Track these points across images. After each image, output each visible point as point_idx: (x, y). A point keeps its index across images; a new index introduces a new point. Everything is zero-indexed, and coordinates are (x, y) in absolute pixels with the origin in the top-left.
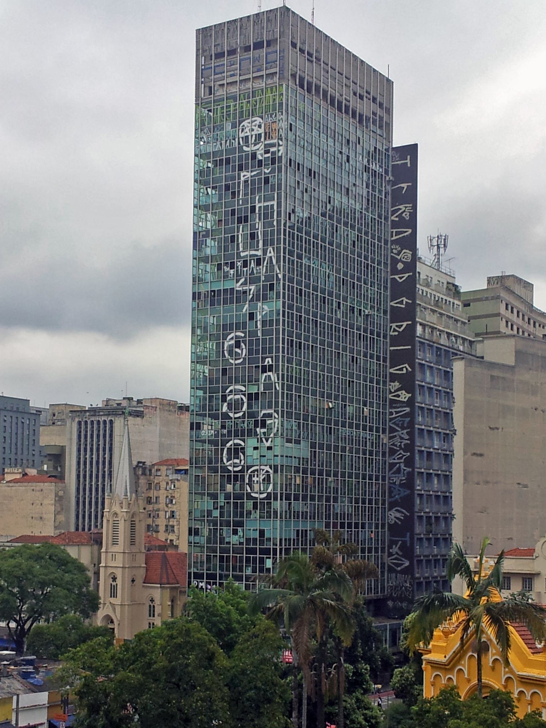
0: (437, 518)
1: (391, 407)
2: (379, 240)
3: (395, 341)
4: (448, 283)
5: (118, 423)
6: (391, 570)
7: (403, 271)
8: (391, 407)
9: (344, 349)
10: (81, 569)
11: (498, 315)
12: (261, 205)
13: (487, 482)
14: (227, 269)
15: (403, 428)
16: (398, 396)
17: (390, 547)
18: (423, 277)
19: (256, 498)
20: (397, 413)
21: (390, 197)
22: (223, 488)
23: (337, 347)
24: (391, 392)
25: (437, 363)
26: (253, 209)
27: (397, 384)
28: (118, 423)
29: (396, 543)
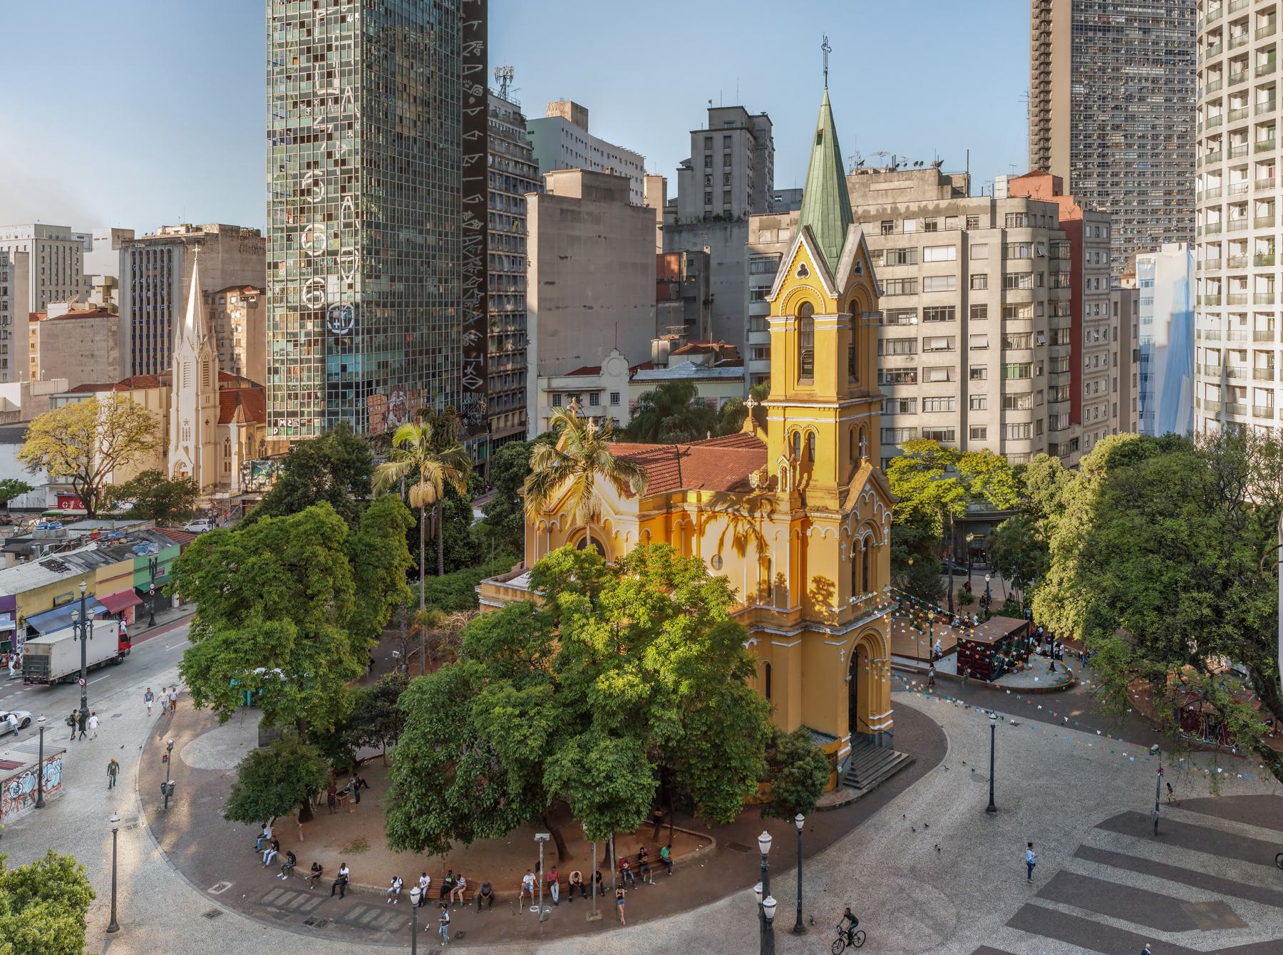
1: (465, 235)
2: (452, 76)
3: (468, 172)
4: (514, 113)
6: (466, 389)
7: (475, 105)
8: (465, 235)
9: (421, 183)
12: (338, 43)
14: (303, 107)
15: (476, 255)
16: (471, 225)
17: (465, 368)
19: (338, 335)
20: (470, 240)
21: (461, 34)
22: (302, 326)
23: (414, 182)
24: (464, 222)
25: (507, 190)
26: (329, 48)
27: (470, 214)
29: (470, 363)
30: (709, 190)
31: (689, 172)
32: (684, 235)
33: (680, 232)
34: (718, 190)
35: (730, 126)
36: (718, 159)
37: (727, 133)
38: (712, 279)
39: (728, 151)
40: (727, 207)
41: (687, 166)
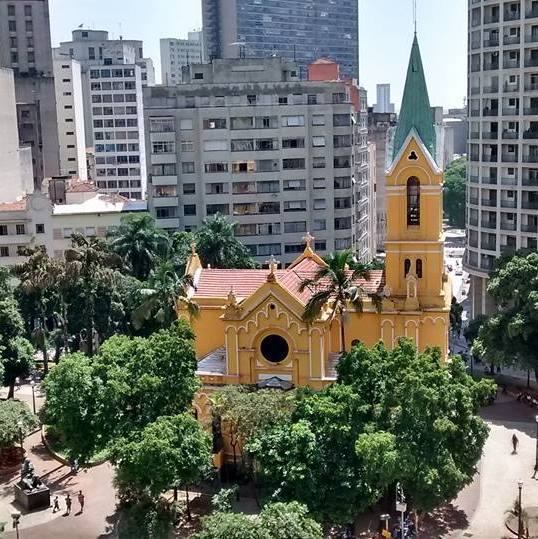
30: (14, 50)
36: (21, 25)
39: (29, 18)
40: (31, 65)
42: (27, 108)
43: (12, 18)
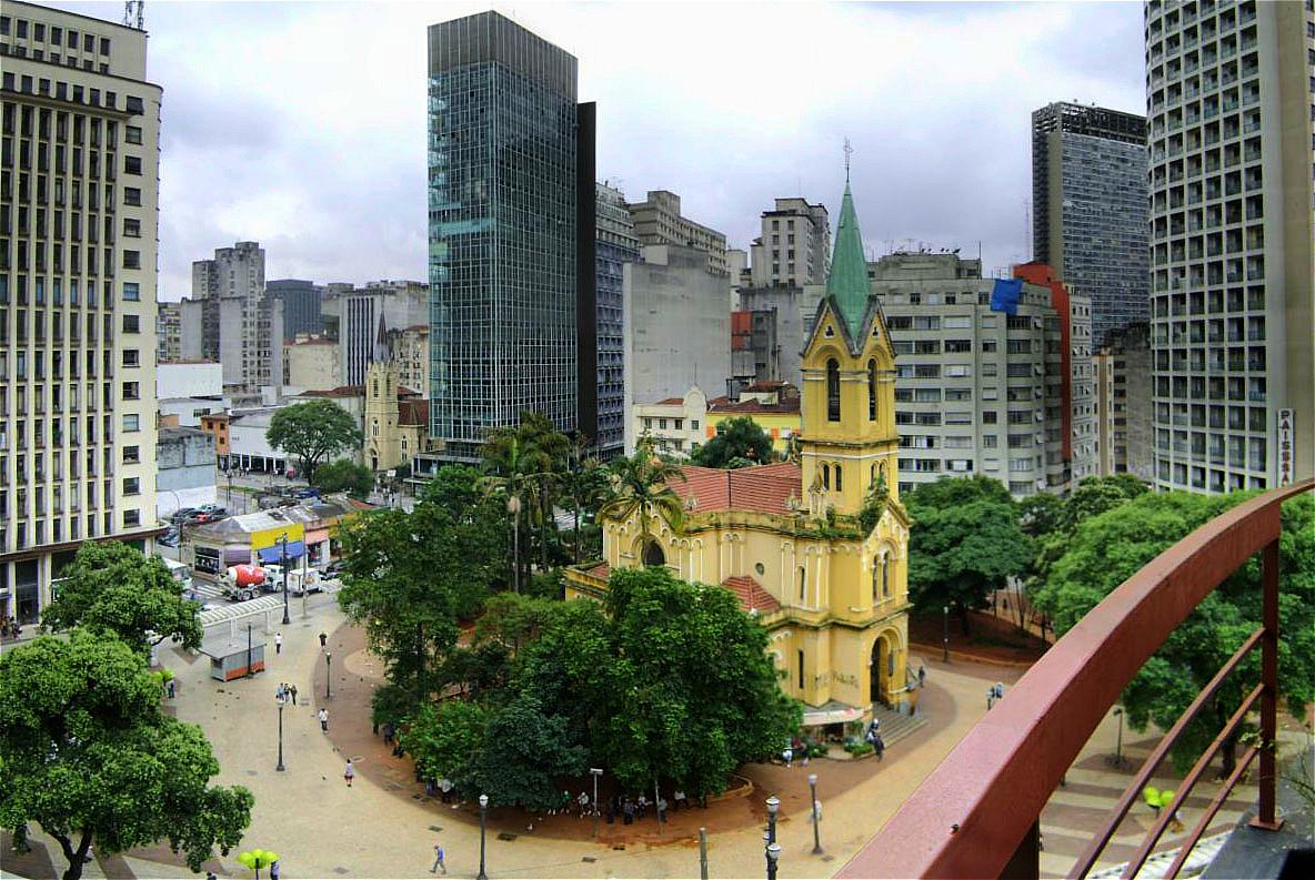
0: (613, 370)
5: (378, 299)
10: (348, 417)
11: (655, 221)
13: (649, 350)
18: (600, 194)
28: (378, 299)
31: (759, 248)
32: (757, 297)
33: (753, 295)
34: (784, 262)
35: (793, 213)
37: (790, 218)
38: (779, 334)
40: (791, 277)
41: (759, 242)
42: (761, 315)
43: (775, 233)
